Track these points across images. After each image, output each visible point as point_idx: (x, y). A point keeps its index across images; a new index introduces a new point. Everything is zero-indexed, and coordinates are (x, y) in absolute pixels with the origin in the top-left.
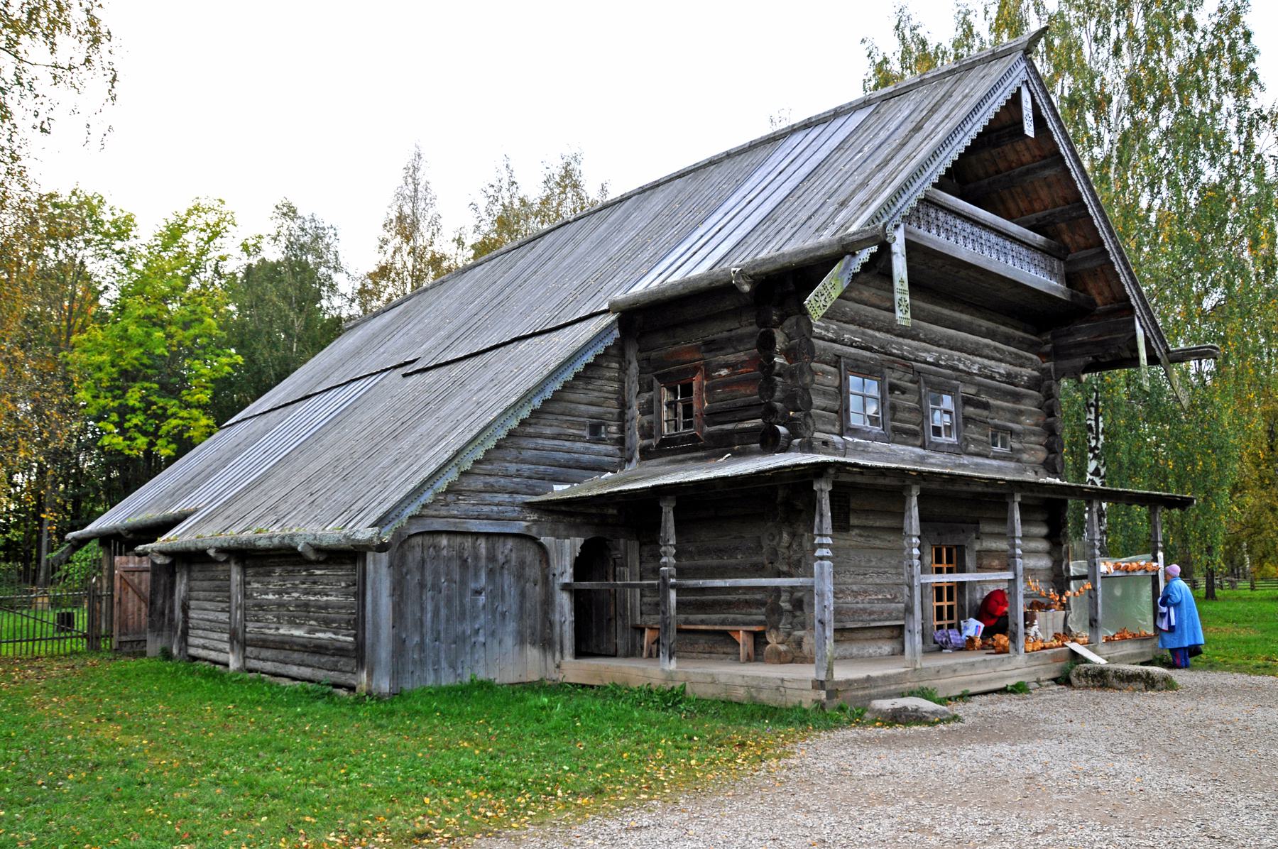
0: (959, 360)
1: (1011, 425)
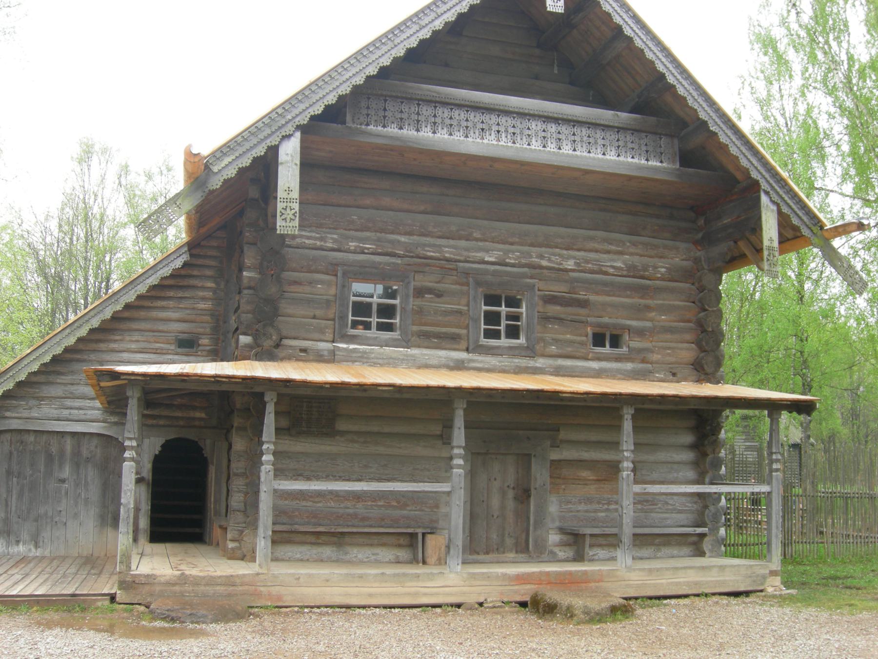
0: (541, 257)
1: (629, 322)
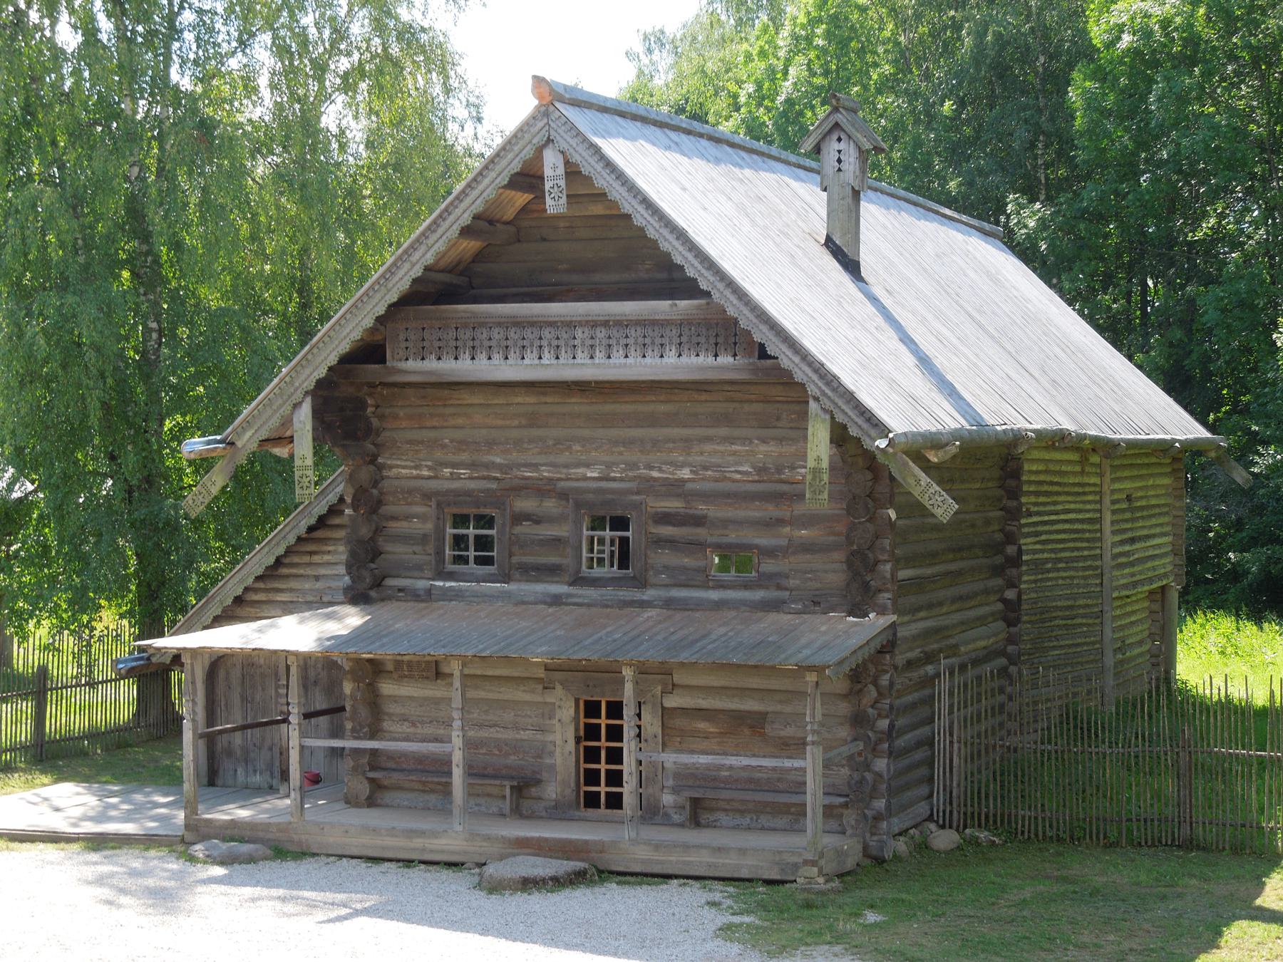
0: (651, 468)
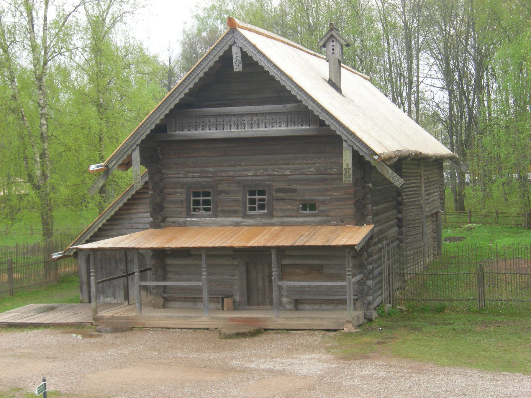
0: (274, 171)
1: (317, 198)
